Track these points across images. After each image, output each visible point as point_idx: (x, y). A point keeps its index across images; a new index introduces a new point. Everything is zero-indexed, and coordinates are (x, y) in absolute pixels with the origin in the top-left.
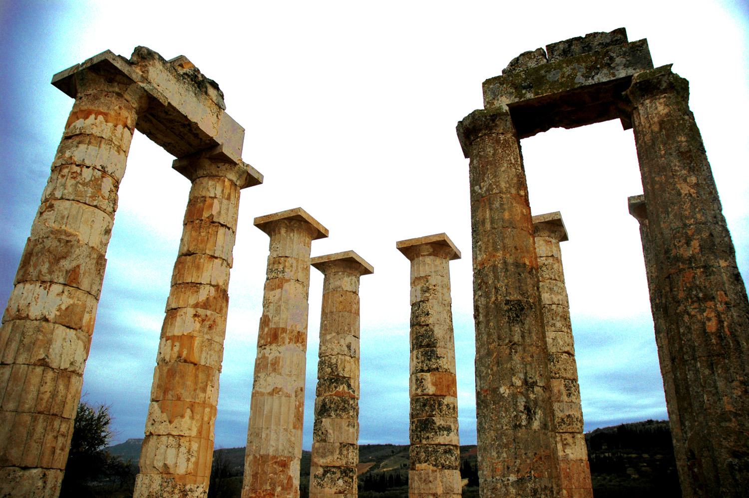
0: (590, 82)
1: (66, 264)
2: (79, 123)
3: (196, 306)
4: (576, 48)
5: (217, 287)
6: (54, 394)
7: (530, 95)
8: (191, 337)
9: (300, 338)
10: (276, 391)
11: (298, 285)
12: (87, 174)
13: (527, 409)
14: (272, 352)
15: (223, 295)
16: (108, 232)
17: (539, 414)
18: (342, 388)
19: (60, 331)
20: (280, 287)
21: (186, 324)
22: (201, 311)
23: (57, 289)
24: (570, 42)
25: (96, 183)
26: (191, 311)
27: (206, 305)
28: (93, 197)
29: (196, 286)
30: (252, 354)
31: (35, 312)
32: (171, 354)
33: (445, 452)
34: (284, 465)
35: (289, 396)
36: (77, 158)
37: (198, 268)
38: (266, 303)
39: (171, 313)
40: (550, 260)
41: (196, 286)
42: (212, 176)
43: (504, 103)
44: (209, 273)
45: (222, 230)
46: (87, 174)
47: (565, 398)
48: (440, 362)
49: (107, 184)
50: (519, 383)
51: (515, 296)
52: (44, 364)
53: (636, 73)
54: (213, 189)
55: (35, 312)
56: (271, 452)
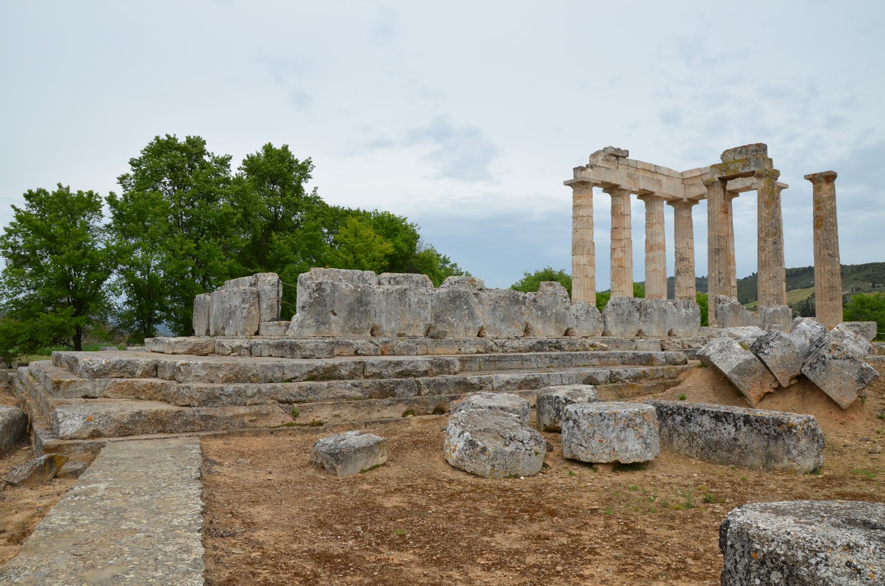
0: (743, 171)
1: (586, 248)
2: (578, 201)
4: (744, 151)
7: (724, 175)
8: (621, 258)
9: (663, 247)
10: (654, 270)
14: (651, 255)
17: (723, 281)
18: (686, 263)
20: (652, 227)
21: (619, 254)
24: (742, 147)
25: (588, 221)
27: (625, 246)
29: (620, 240)
30: (644, 255)
31: (581, 263)
32: (616, 264)
36: (581, 214)
38: (647, 234)
39: (613, 250)
41: (620, 240)
43: (716, 177)
46: (585, 219)
50: (717, 272)
51: (717, 247)
53: (757, 170)
54: (620, 201)
55: (581, 263)
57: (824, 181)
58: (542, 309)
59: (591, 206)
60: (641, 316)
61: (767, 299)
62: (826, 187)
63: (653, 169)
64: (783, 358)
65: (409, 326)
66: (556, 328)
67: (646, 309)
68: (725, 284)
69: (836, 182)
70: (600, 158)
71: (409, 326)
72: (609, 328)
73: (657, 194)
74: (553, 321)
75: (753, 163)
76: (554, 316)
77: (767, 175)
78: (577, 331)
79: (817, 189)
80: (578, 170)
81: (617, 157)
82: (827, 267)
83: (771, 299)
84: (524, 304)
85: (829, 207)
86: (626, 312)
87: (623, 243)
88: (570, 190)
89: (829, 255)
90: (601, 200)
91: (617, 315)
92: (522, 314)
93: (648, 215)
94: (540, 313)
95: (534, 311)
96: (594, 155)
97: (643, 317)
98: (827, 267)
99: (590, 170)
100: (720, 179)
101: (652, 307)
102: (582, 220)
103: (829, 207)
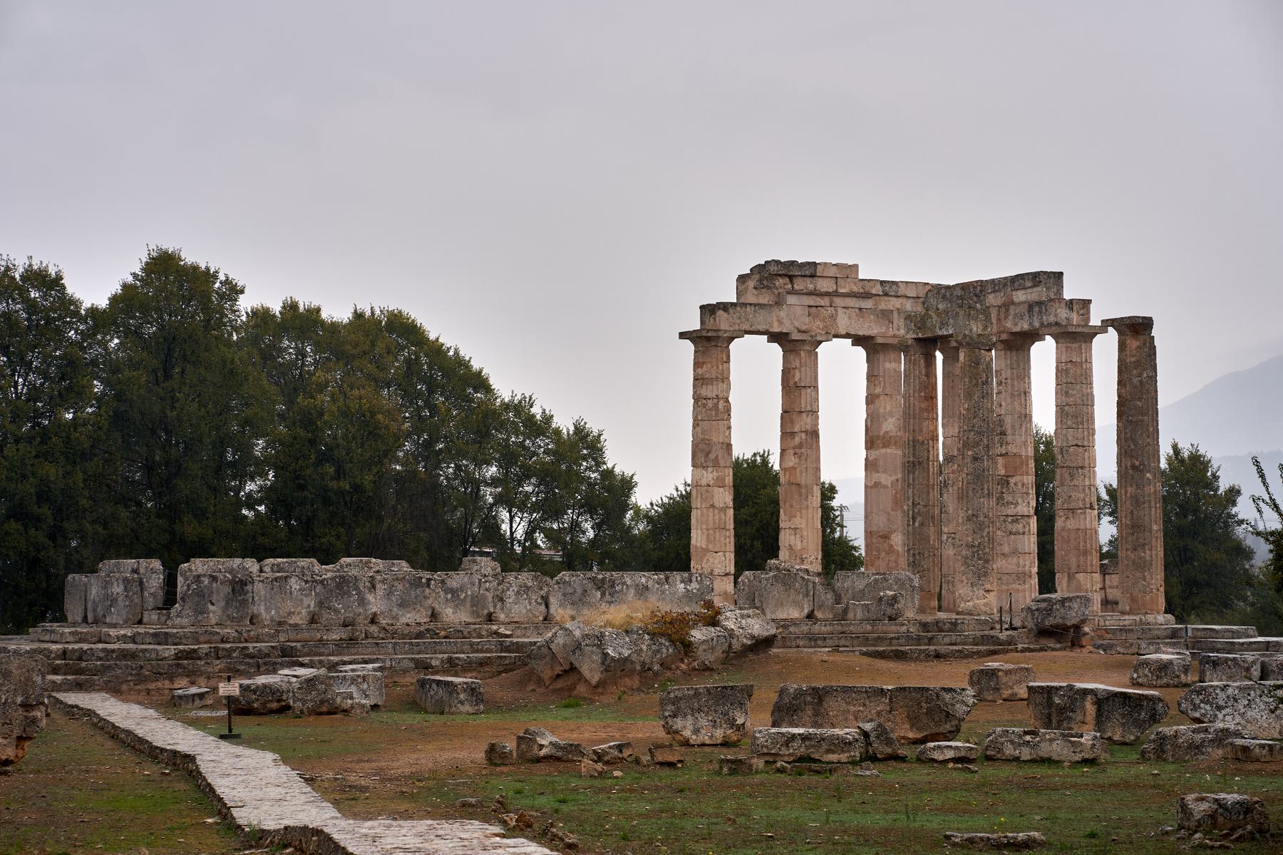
0: (940, 333)
1: (712, 456)
2: (700, 371)
3: (794, 448)
5: (806, 432)
6: (720, 519)
8: (793, 468)
10: (877, 485)
11: (888, 399)
12: (710, 403)
13: (914, 519)
15: (814, 434)
16: (729, 428)
19: (716, 489)
22: (798, 451)
23: (710, 469)
25: (716, 406)
26: (792, 452)
27: (801, 446)
28: (716, 415)
29: (793, 434)
31: (704, 482)
33: (1013, 521)
34: (886, 537)
35: (885, 487)
37: (792, 422)
40: (1069, 366)
41: (793, 434)
42: (792, 351)
44: (803, 423)
45: (803, 391)
46: (710, 403)
47: (1067, 482)
48: (1009, 447)
49: (721, 404)
52: (713, 506)
56: (875, 529)
57: (1136, 331)
58: (453, 592)
59: (725, 378)
60: (603, 595)
61: (964, 553)
62: (1133, 344)
63: (877, 290)
64: (564, 645)
65: (290, 613)
66: (473, 613)
67: (613, 586)
68: (922, 524)
69: (1155, 332)
70: (751, 284)
71: (290, 613)
72: (552, 610)
73: (880, 340)
74: (468, 605)
75: (951, 321)
76: (469, 599)
77: (968, 344)
78: (502, 617)
79: (1122, 347)
80: (708, 311)
81: (791, 278)
82: (1129, 489)
83: (969, 553)
84: (428, 586)
85: (1135, 380)
86: (579, 591)
87: (797, 440)
88: (689, 346)
89: (1133, 467)
90: (755, 364)
91: (564, 595)
92: (426, 598)
93: (871, 377)
94: (449, 596)
95: (442, 594)
96: (742, 279)
97: (608, 597)
98: (1129, 489)
99: (720, 312)
100: (918, 340)
101: (624, 583)
102: (704, 406)
103: (1135, 380)
